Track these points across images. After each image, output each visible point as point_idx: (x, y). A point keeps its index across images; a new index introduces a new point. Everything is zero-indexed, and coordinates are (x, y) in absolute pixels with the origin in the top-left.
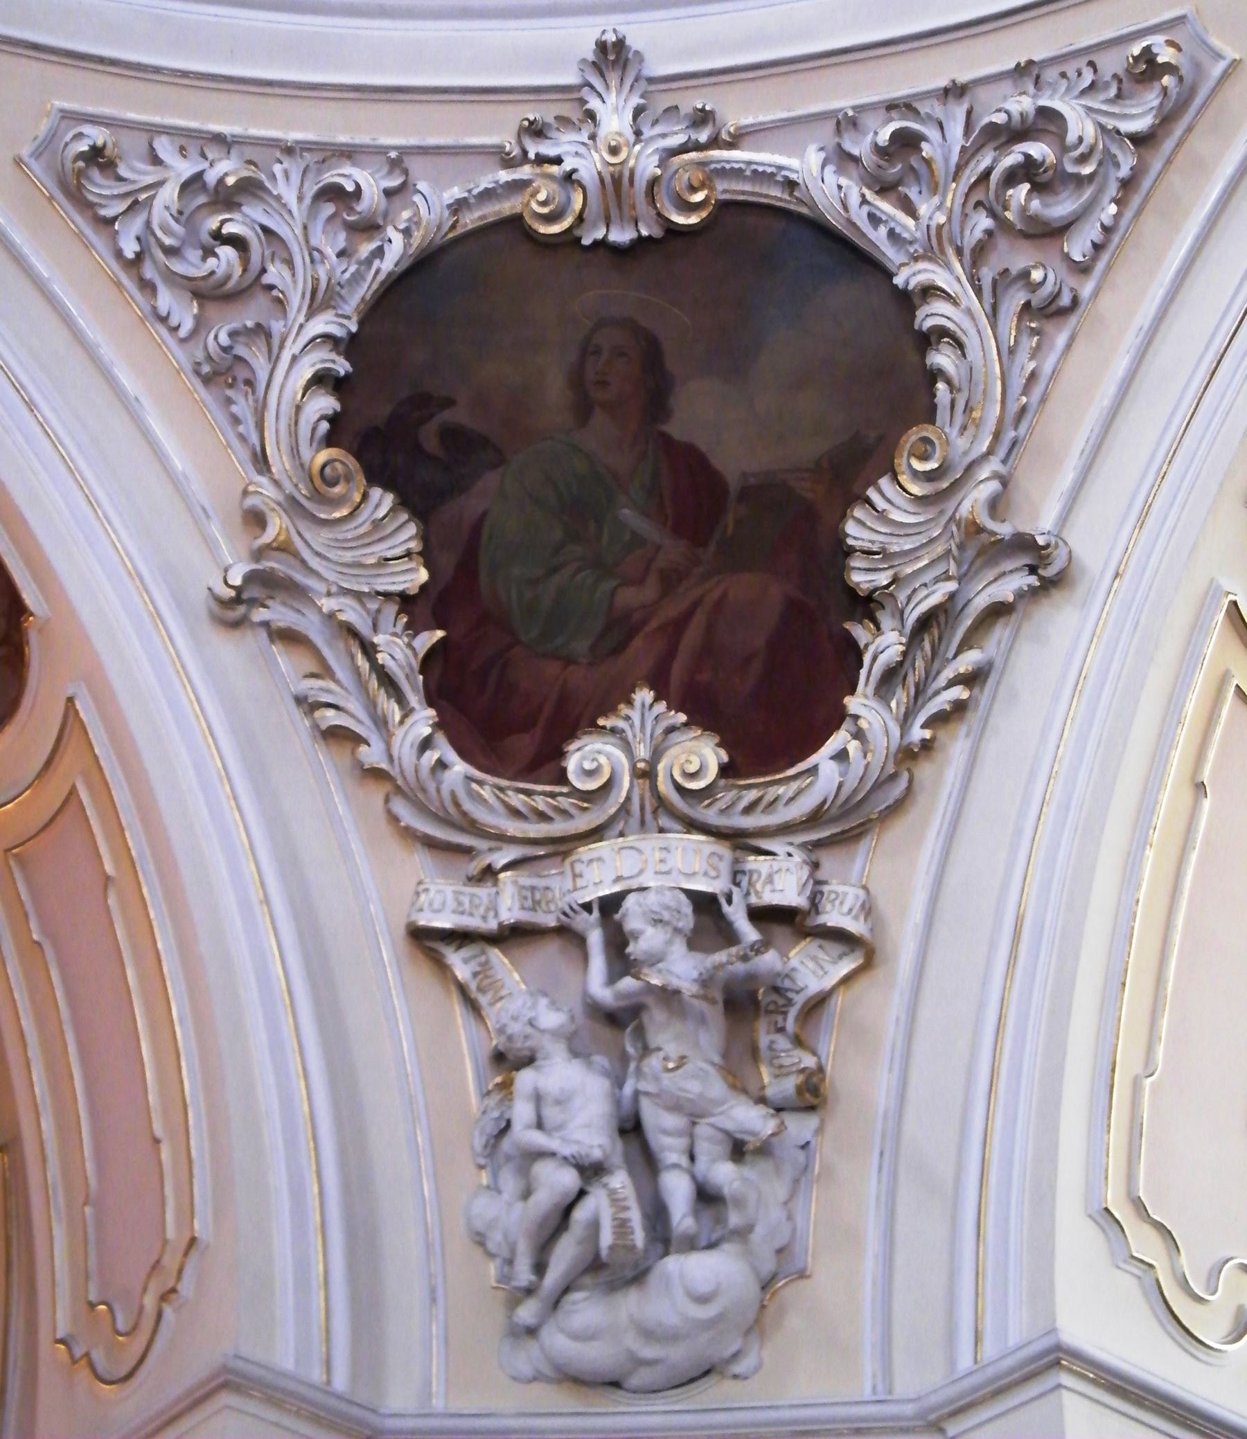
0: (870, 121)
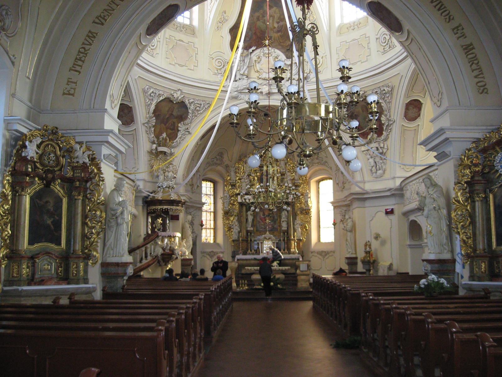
0: (374, 90)
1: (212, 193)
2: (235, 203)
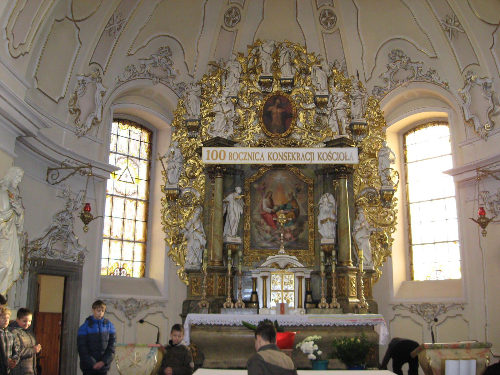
1: (145, 155)
2: (197, 174)
